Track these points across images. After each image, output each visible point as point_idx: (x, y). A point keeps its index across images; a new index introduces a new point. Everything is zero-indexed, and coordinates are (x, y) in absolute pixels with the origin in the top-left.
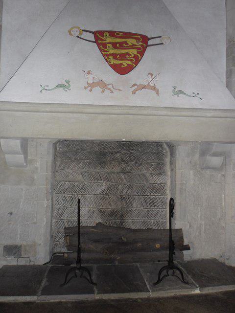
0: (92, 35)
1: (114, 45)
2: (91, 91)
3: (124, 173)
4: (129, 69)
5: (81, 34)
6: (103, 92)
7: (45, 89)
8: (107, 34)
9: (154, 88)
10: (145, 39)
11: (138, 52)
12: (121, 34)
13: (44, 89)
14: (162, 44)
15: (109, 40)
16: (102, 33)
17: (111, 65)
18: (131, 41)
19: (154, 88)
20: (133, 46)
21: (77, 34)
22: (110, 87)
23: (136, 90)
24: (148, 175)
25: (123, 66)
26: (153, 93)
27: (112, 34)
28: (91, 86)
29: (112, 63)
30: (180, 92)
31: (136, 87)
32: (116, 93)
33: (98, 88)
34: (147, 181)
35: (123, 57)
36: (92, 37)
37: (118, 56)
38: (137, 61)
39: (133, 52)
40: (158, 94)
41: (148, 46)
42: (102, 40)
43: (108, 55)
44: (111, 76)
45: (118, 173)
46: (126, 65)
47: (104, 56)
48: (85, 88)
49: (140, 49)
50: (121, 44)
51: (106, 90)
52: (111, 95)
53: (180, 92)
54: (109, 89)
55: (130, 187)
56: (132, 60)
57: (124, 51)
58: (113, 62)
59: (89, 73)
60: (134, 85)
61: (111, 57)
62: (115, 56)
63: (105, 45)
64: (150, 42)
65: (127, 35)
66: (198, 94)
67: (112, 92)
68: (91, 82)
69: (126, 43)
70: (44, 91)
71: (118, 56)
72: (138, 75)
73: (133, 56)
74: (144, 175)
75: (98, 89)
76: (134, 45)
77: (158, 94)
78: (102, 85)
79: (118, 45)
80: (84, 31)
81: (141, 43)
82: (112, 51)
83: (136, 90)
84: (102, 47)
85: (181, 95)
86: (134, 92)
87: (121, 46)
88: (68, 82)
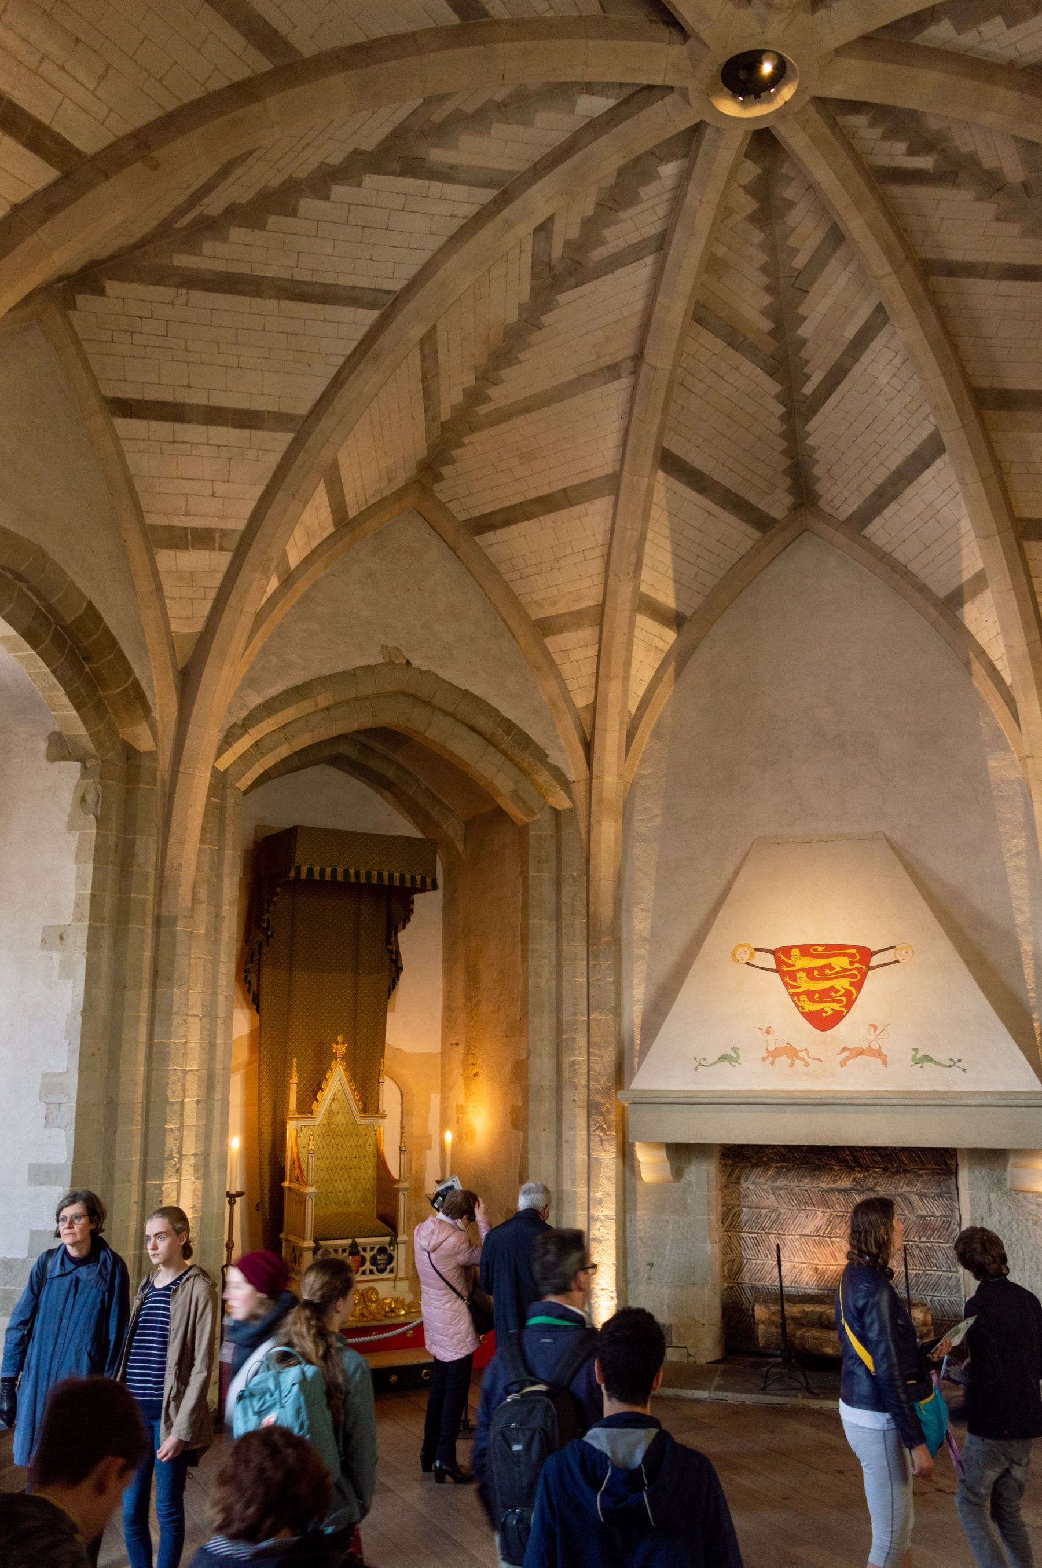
0: (771, 957)
2: (772, 1063)
4: (837, 1017)
5: (752, 957)
6: (792, 1065)
7: (701, 1064)
8: (796, 952)
9: (878, 1054)
10: (866, 954)
11: (852, 984)
12: (820, 949)
13: (700, 1064)
14: (897, 961)
15: (800, 962)
16: (787, 950)
17: (804, 1014)
18: (840, 962)
19: (878, 1054)
20: (843, 973)
21: (746, 959)
22: (803, 1055)
23: (848, 1059)
25: (824, 1015)
26: (879, 1061)
27: (806, 950)
29: (806, 1010)
30: (927, 1058)
31: (847, 1053)
33: (784, 1058)
35: (825, 995)
36: (770, 961)
37: (817, 995)
40: (885, 1063)
41: (870, 968)
42: (789, 965)
43: (798, 995)
46: (830, 1012)
47: (792, 995)
48: (764, 1059)
49: (854, 976)
50: (821, 969)
51: (798, 1063)
52: (805, 1069)
53: (927, 1058)
54: (803, 1059)
56: (839, 1002)
59: (768, 1032)
60: (845, 1049)
61: (804, 998)
62: (810, 994)
63: (793, 975)
64: (874, 961)
65: (833, 950)
66: (959, 1061)
67: (807, 1065)
68: (772, 1048)
69: (829, 966)
70: (700, 1068)
71: (817, 995)
73: (842, 991)
75: (784, 1059)
76: (844, 970)
77: (885, 1063)
79: (816, 973)
80: (757, 950)
81: (856, 965)
83: (848, 1059)
84: (788, 976)
85: (926, 1064)
86: (843, 1063)
87: (822, 973)
88: (735, 1050)
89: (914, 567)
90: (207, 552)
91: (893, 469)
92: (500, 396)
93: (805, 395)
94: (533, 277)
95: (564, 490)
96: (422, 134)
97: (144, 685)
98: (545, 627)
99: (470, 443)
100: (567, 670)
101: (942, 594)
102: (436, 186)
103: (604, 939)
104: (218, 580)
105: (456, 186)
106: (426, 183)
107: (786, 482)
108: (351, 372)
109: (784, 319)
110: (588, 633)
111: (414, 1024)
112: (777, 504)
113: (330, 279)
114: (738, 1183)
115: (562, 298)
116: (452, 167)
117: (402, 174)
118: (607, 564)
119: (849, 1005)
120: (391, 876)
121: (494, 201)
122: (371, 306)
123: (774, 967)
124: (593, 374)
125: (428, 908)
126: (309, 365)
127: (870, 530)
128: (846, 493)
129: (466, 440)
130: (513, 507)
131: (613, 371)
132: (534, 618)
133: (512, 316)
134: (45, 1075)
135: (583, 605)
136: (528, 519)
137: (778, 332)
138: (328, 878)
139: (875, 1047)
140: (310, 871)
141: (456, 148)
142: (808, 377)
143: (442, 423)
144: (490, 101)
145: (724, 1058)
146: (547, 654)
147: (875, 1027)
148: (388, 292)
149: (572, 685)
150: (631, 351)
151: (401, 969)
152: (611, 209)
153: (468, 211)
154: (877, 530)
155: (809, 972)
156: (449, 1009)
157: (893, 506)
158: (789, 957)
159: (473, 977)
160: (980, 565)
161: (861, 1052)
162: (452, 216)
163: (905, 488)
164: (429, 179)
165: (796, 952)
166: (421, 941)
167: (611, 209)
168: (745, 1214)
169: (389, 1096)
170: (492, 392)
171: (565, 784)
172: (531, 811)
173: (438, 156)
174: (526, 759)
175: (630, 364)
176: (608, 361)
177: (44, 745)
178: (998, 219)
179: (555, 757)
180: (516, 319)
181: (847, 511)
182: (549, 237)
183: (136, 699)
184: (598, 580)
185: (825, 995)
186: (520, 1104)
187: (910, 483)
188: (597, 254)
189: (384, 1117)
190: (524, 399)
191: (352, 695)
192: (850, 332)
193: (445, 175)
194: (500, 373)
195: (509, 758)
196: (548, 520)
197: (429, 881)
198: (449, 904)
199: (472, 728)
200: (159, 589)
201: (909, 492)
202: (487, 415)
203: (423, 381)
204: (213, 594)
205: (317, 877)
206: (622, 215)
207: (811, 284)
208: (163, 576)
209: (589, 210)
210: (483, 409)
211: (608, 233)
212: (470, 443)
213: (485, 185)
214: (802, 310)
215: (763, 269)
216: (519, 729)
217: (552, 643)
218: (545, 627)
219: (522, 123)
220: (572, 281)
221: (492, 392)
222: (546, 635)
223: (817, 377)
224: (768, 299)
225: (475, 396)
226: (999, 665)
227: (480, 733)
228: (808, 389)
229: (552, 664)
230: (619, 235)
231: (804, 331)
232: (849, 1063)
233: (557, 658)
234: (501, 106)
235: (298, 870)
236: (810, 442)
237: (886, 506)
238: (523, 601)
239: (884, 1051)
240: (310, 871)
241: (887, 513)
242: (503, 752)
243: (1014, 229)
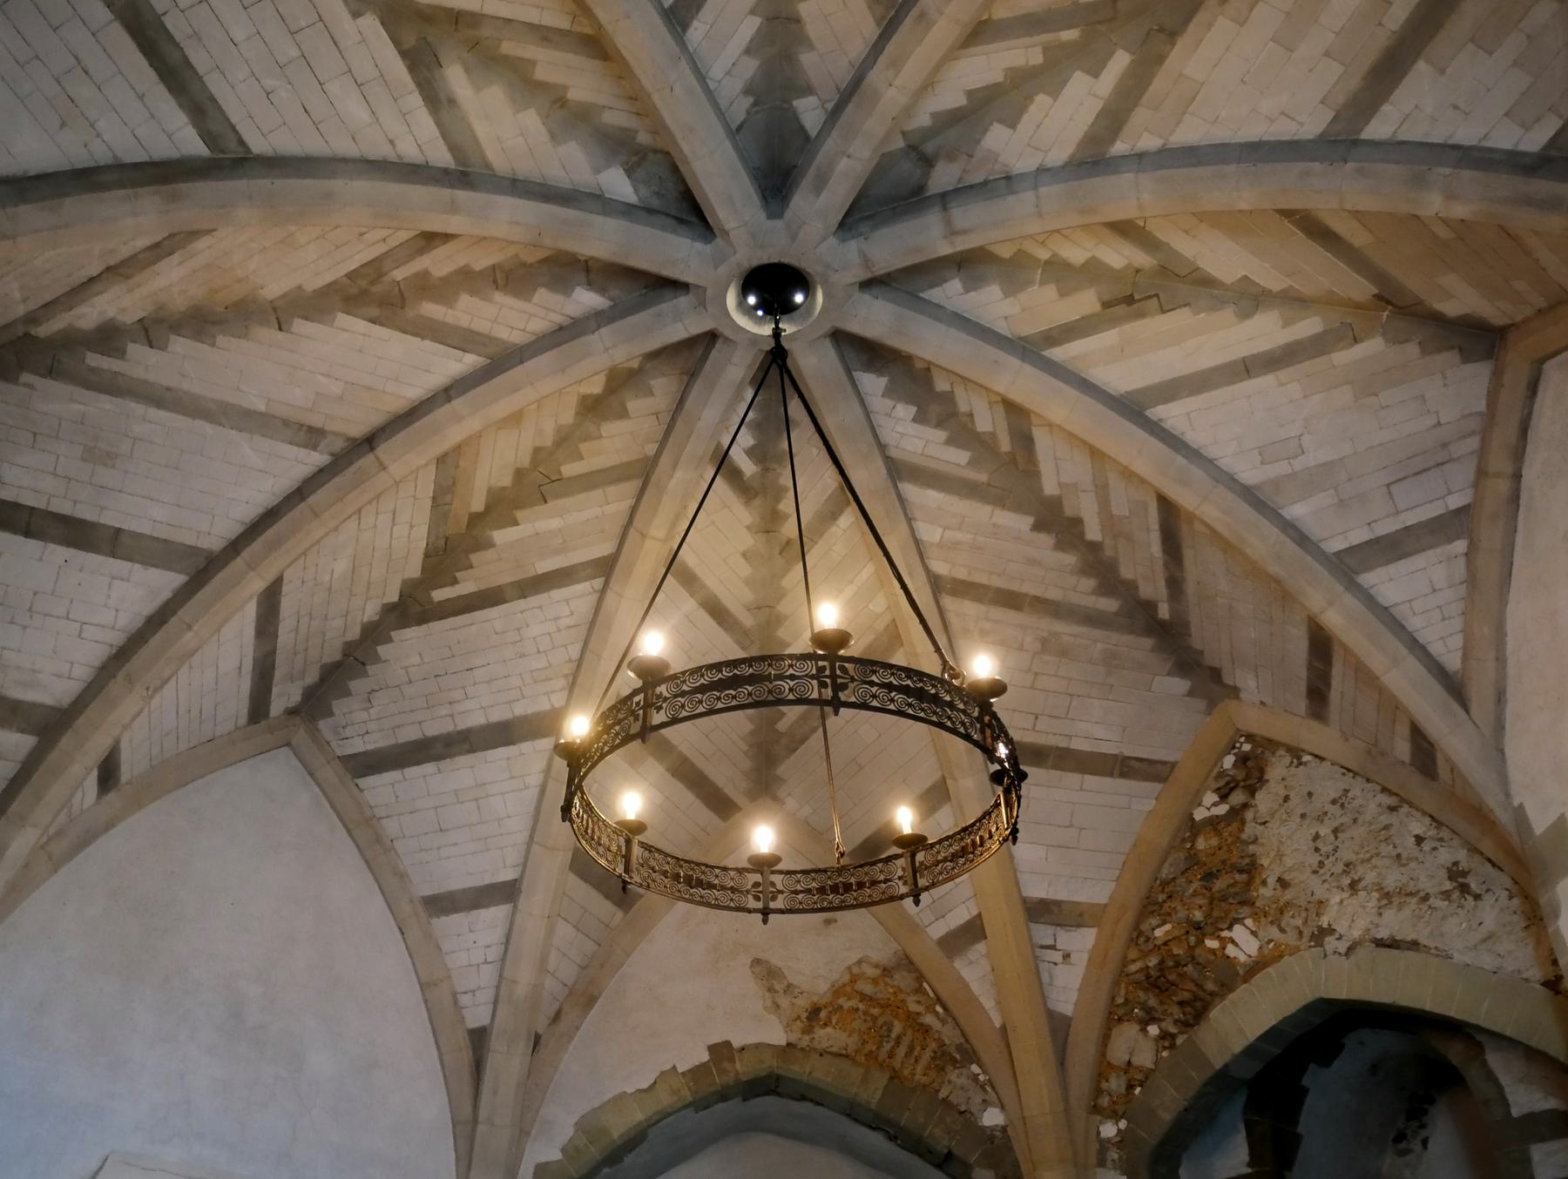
91: (461, 727)
92: (141, 362)
93: (430, 597)
94: (349, 276)
95: (118, 531)
96: (474, 45)
99: (30, 386)
102: (415, 100)
105: (431, 121)
106: (411, 85)
107: (312, 677)
108: (121, 185)
109: (502, 507)
112: (285, 695)
113: (199, 60)
115: (343, 319)
116: (452, 102)
117: (404, 54)
121: (446, 171)
122: (208, 137)
124: (286, 423)
126: (63, 125)
127: (368, 782)
128: (372, 726)
129: (26, 377)
130: (16, 506)
131: (312, 436)
133: (273, 289)
136: (27, 534)
137: (475, 519)
141: (478, 88)
142: (455, 582)
143: (27, 335)
144: (565, 88)
148: (242, 142)
150: (358, 430)
152: (495, 282)
153: (408, 150)
154: (380, 788)
157: (429, 768)
162: (392, 142)
163: (460, 754)
164: (419, 85)
167: (495, 282)
170: (136, 350)
173: (455, 78)
175: (339, 445)
176: (316, 420)
178: (744, 555)
180: (270, 297)
181: (357, 746)
182: (421, 252)
187: (472, 751)
188: (432, 310)
190: (169, 389)
192: (544, 566)
193: (436, 99)
194: (173, 337)
196: (58, 553)
201: (463, 760)
202: (93, 370)
203: (108, 269)
206: (498, 297)
207: (557, 497)
209: (478, 267)
210: (94, 360)
211: (465, 300)
212: (30, 386)
213: (453, 148)
214: (519, 514)
215: (537, 451)
219: (553, 137)
220: (374, 312)
221: (136, 350)
223: (466, 586)
224: (506, 481)
225: (108, 338)
228: (439, 595)
230: (470, 312)
231: (500, 536)
234: (561, 102)
236: (381, 649)
237: (418, 763)
241: (413, 771)
243: (745, 570)
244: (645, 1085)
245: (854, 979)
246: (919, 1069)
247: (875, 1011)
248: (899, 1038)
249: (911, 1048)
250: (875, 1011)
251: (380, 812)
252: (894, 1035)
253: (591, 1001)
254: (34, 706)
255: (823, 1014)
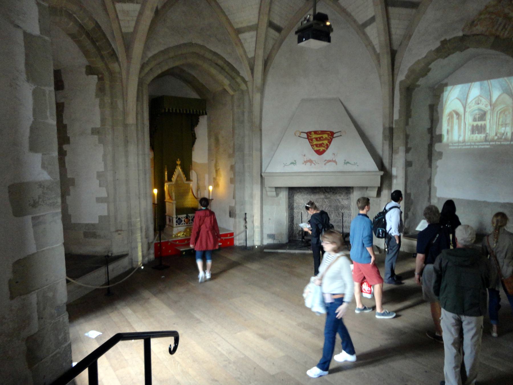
1: (316, 139)
3: (326, 199)
4: (324, 151)
5: (300, 134)
7: (285, 165)
8: (313, 133)
9: (335, 162)
10: (332, 134)
15: (314, 136)
16: (310, 133)
18: (325, 136)
19: (335, 162)
21: (299, 135)
22: (314, 162)
24: (340, 200)
26: (334, 164)
27: (316, 132)
28: (305, 162)
30: (348, 163)
32: (317, 165)
34: (340, 202)
35: (321, 145)
36: (305, 136)
38: (327, 147)
39: (326, 142)
40: (336, 164)
41: (333, 137)
44: (315, 157)
45: (323, 199)
46: (322, 150)
47: (311, 145)
49: (328, 140)
50: (320, 138)
53: (348, 163)
55: (330, 206)
56: (324, 147)
57: (321, 142)
58: (316, 149)
59: (304, 156)
60: (325, 160)
61: (315, 146)
62: (316, 145)
63: (312, 140)
64: (335, 136)
65: (323, 132)
68: (305, 160)
69: (322, 137)
72: (328, 155)
74: (338, 200)
75: (308, 164)
77: (336, 164)
78: (311, 161)
82: (315, 142)
84: (310, 140)
85: (348, 164)
86: (325, 164)
87: (320, 139)
88: (295, 161)
89: (353, 14)
90: (132, 4)
97: (115, 50)
98: (239, 31)
100: (246, 45)
101: (360, 23)
103: (258, 129)
104: (137, 14)
110: (253, 33)
111: (200, 155)
114: (293, 197)
118: (260, 10)
119: (327, 148)
120: (193, 111)
123: (306, 137)
125: (203, 121)
132: (236, 27)
134: (98, 172)
135: (251, 24)
138: (174, 111)
139: (334, 159)
140: (169, 110)
145: (292, 163)
146: (240, 40)
147: (334, 154)
149: (247, 50)
151: (196, 138)
155: (316, 139)
156: (210, 150)
158: (311, 134)
159: (217, 140)
160: (373, 14)
161: (329, 161)
165: (313, 133)
166: (202, 130)
168: (295, 205)
169: (193, 175)
171: (245, 82)
172: (234, 90)
174: (234, 74)
177: (84, 70)
179: (242, 74)
183: (113, 55)
184: (257, 15)
185: (321, 145)
186: (232, 176)
189: (192, 181)
191: (180, 53)
195: (228, 74)
197: (204, 112)
198: (209, 119)
199: (217, 64)
200: (117, 17)
204: (135, 19)
205: (171, 111)
208: (118, 12)
216: (232, 65)
217: (241, 36)
218: (239, 31)
222: (239, 34)
226: (376, 47)
227: (219, 66)
229: (241, 43)
232: (328, 164)
233: (243, 41)
235: (165, 109)
238: (232, 22)
239: (337, 160)
240: (169, 110)
242: (227, 72)
244: (424, 56)
245: (487, 7)
246: (507, 32)
247: (493, 17)
248: (500, 24)
249: (504, 26)
250: (493, 17)
251: (345, 7)
252: (499, 23)
253: (410, 37)
254: (252, 25)
255: (475, 22)
